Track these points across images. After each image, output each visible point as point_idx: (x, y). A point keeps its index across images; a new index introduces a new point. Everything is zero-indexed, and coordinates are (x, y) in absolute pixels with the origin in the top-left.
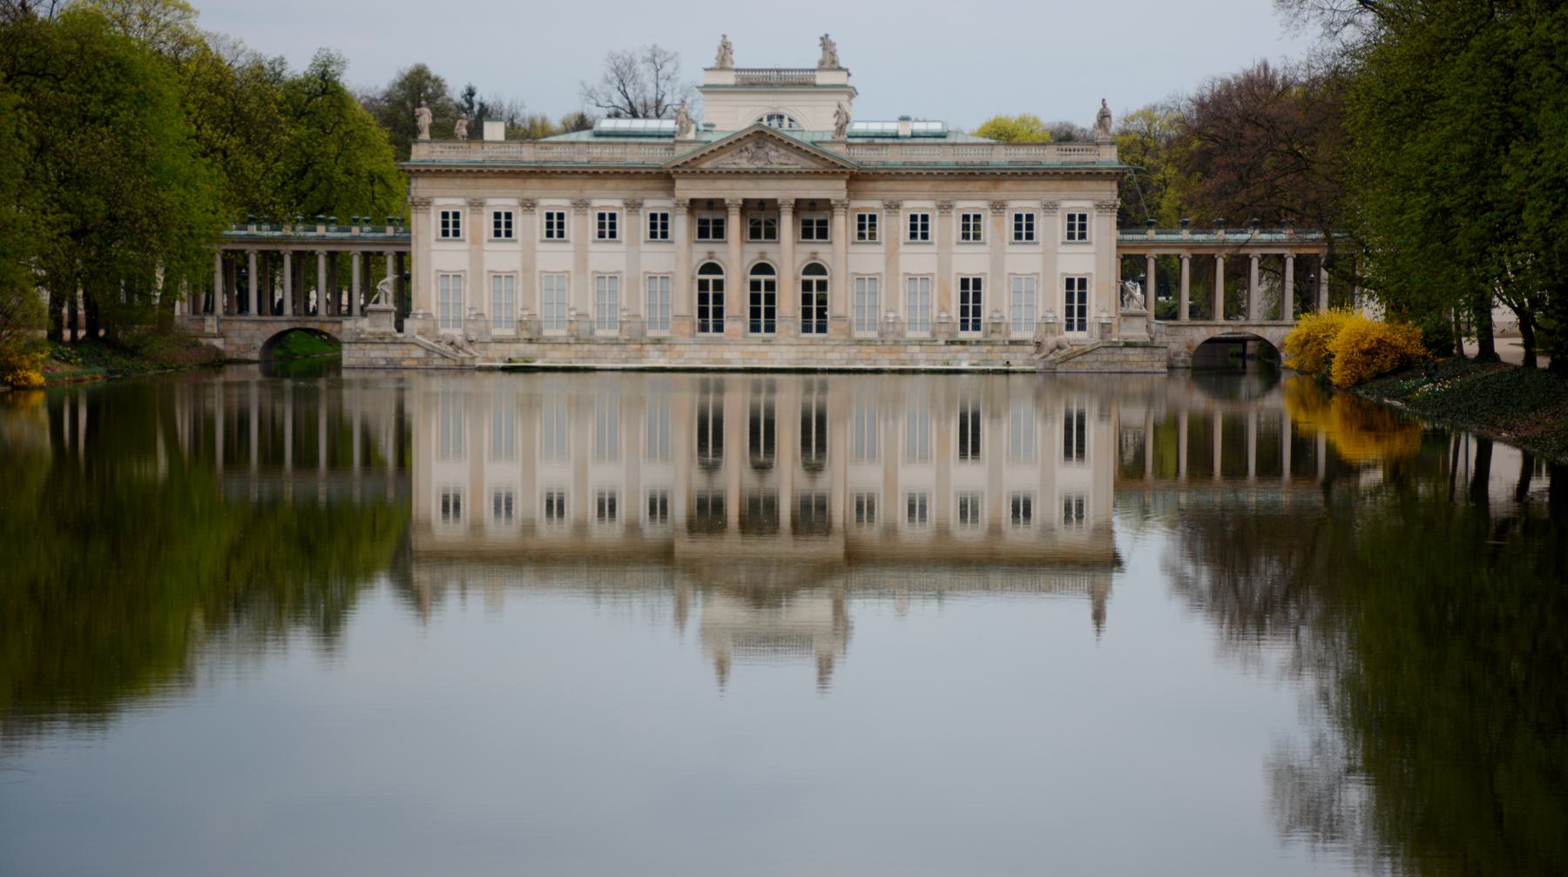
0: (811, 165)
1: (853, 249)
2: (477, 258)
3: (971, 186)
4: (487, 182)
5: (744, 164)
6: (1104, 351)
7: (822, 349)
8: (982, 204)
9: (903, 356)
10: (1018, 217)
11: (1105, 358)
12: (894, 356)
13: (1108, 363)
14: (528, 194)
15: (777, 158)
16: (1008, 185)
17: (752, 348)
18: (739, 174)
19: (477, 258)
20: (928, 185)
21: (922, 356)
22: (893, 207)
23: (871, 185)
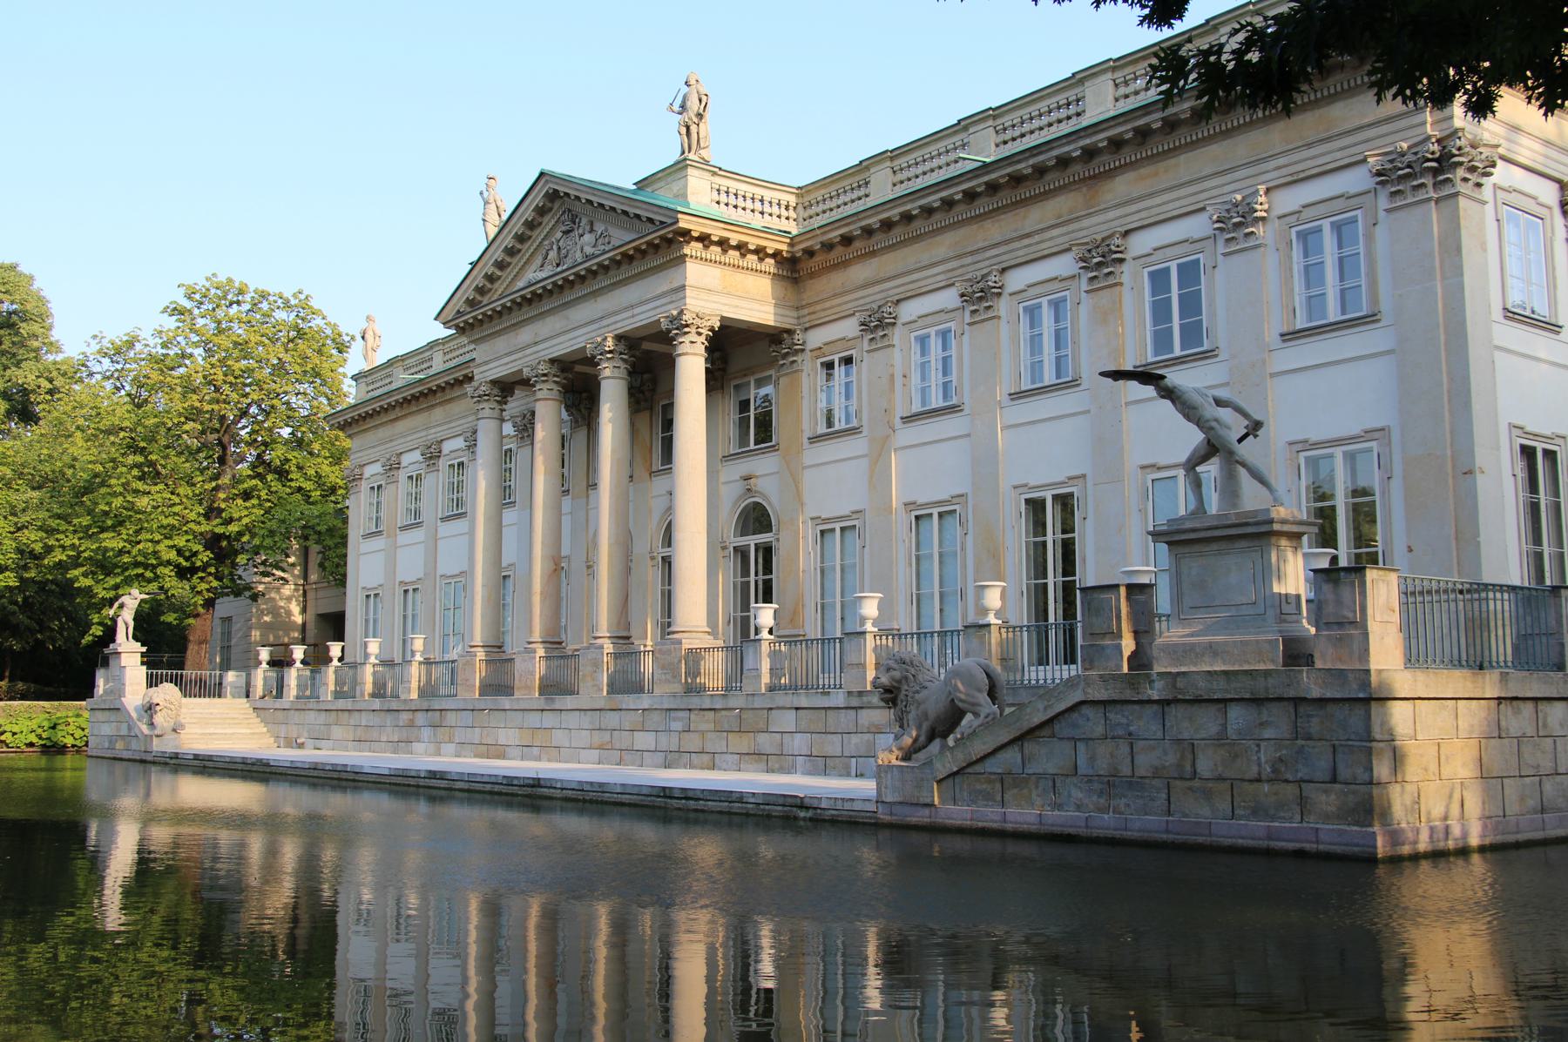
0: (621, 237)
1: (814, 454)
2: (391, 565)
3: (1035, 216)
4: (401, 426)
5: (535, 274)
6: (1093, 722)
7: (629, 720)
8: (1065, 265)
9: (765, 742)
10: (1159, 280)
11: (1105, 757)
12: (743, 743)
13: (1110, 785)
14: (434, 434)
15: (586, 246)
16: (1123, 185)
17: (534, 719)
18: (534, 301)
19: (391, 565)
20: (943, 246)
21: (799, 743)
22: (878, 325)
23: (837, 280)
